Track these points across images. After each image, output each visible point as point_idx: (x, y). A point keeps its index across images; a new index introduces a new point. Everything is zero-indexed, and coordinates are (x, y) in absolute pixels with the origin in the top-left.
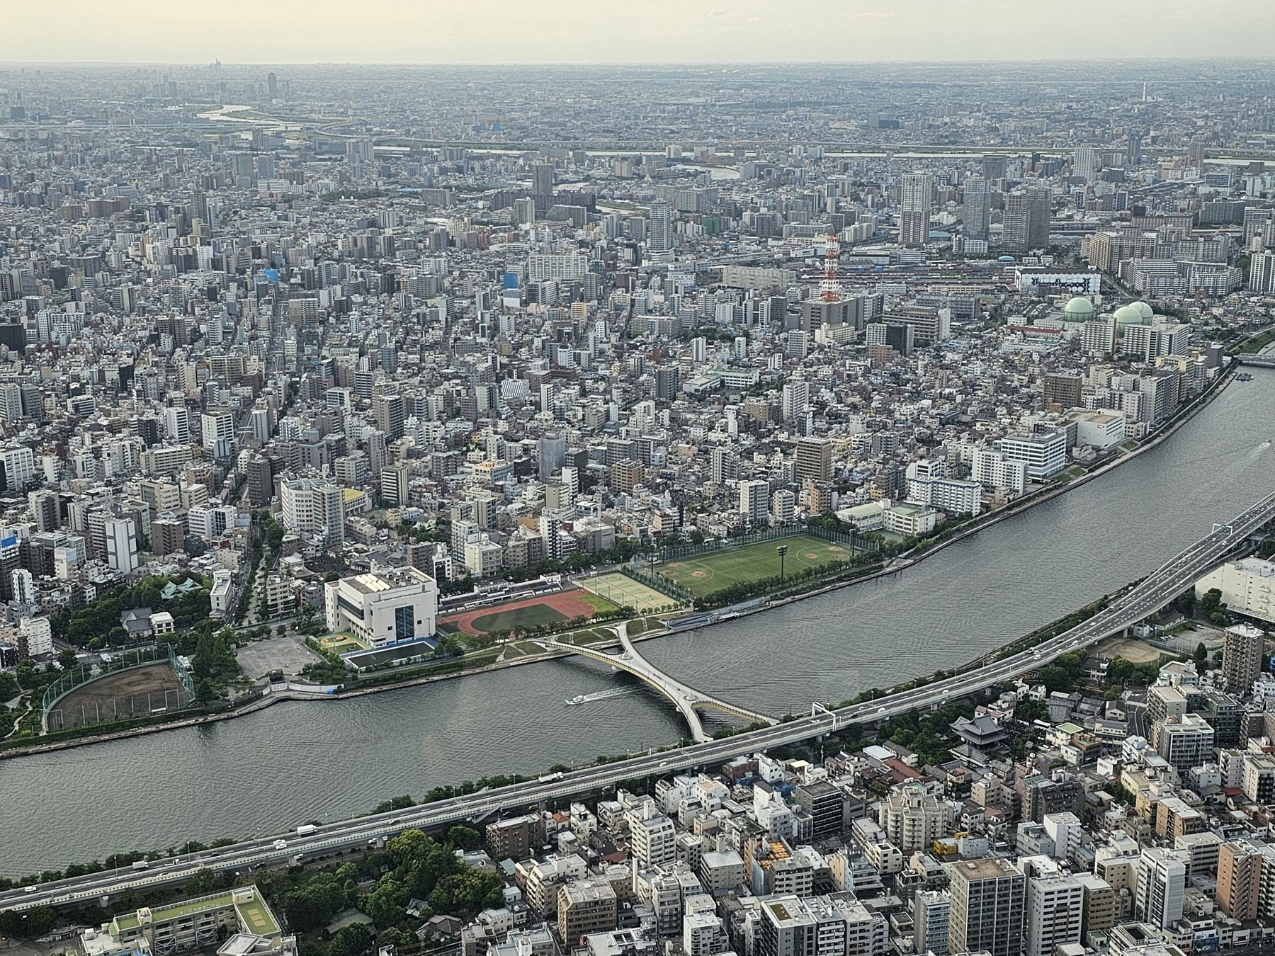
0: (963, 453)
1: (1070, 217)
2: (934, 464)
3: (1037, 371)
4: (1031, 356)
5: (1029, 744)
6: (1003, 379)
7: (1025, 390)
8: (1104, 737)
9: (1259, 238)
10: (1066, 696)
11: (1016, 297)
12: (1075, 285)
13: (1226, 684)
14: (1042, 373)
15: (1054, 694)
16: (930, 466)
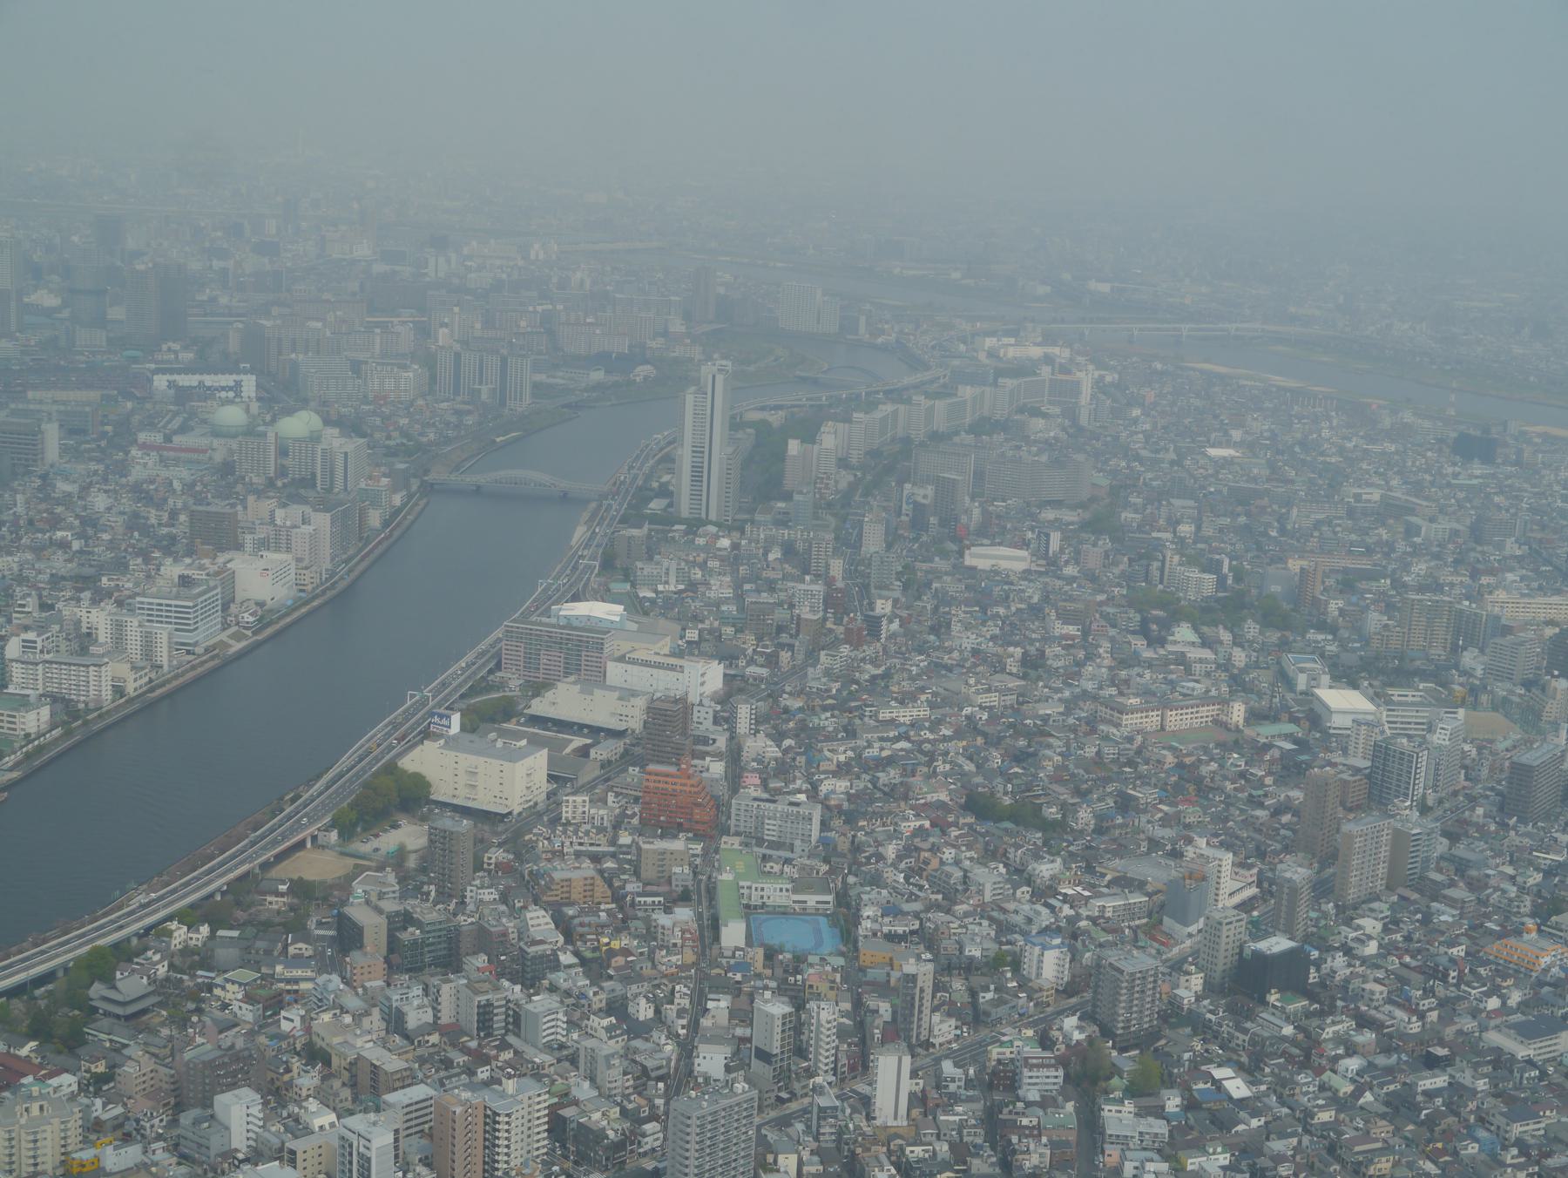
0: (84, 620)
1: (213, 300)
2: (44, 637)
3: (179, 505)
4: (171, 484)
5: (191, 1006)
6: (136, 515)
7: (165, 531)
8: (288, 981)
10: (235, 933)
11: (148, 406)
12: (223, 389)
13: (433, 894)
14: (185, 507)
15: (221, 933)
16: (39, 640)
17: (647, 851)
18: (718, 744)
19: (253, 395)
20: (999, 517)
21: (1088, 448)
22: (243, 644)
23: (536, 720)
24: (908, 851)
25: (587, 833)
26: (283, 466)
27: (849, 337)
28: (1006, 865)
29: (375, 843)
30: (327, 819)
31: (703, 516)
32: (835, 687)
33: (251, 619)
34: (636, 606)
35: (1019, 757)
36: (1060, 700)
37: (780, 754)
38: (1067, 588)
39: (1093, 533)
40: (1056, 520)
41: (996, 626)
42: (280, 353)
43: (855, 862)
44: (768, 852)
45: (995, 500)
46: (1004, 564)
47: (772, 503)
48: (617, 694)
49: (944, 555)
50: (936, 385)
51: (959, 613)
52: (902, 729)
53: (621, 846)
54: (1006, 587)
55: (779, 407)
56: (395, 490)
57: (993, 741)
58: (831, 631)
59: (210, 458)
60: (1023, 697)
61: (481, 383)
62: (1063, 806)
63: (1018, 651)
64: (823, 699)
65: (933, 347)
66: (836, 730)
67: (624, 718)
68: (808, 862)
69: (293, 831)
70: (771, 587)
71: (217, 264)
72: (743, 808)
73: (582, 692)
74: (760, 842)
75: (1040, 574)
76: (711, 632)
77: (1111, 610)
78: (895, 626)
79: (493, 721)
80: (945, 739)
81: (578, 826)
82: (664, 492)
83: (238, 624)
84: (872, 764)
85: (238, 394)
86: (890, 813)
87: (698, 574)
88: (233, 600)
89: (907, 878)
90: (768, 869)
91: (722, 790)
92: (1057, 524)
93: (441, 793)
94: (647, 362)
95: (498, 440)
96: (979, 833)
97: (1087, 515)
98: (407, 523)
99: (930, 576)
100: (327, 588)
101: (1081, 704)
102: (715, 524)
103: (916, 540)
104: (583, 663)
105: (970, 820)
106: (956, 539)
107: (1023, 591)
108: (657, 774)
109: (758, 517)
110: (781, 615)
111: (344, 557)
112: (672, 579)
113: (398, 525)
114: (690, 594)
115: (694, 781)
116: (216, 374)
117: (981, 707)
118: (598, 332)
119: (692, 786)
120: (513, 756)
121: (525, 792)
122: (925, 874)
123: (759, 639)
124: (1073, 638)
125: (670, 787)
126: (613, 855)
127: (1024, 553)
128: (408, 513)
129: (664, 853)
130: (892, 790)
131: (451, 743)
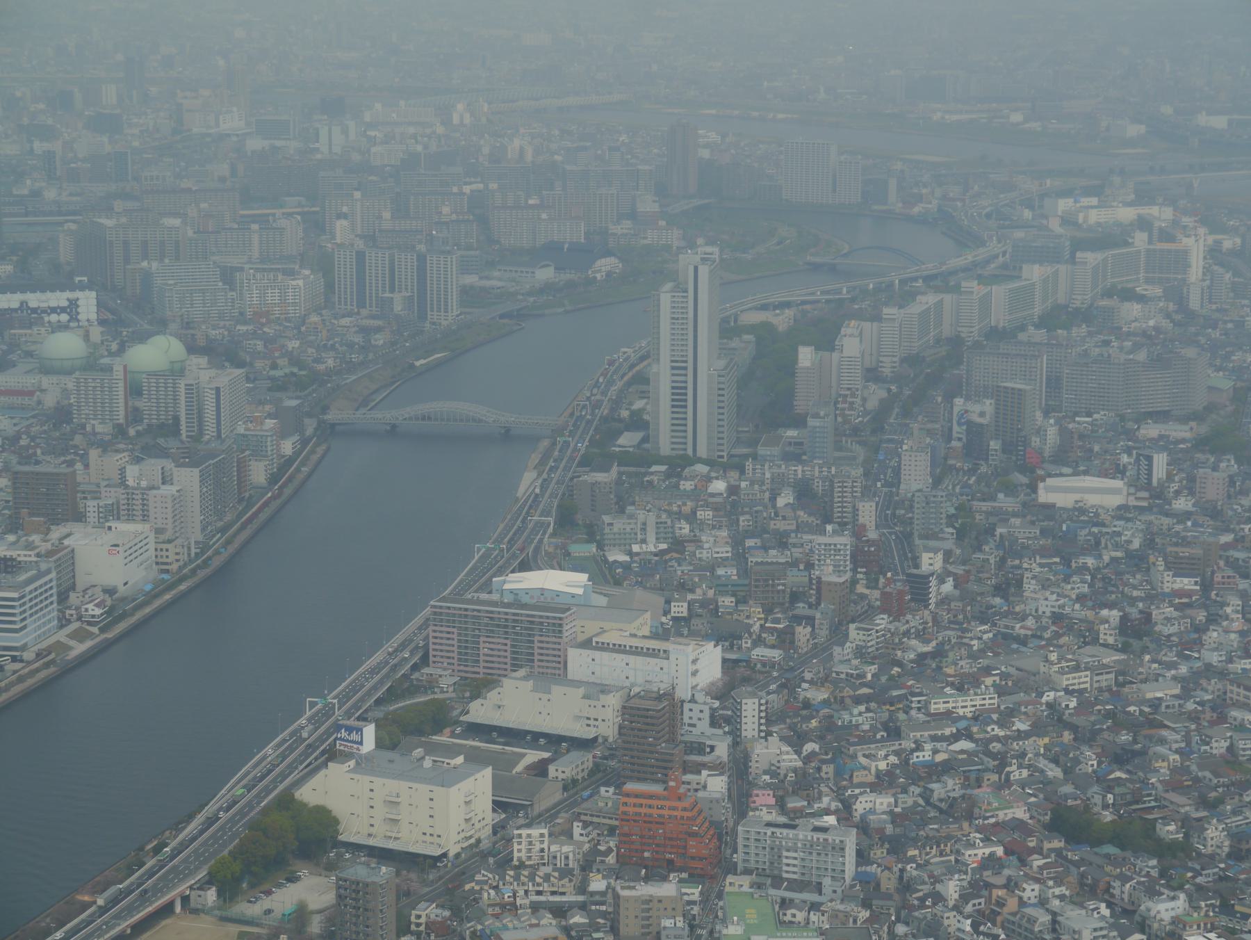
1: (36, 194)
9: (344, 223)
12: (54, 310)
17: (627, 899)
18: (717, 752)
19: (93, 317)
20: (1082, 437)
21: (1202, 340)
22: (89, 644)
23: (477, 730)
24: (976, 888)
25: (547, 878)
26: (136, 409)
27: (876, 207)
28: (1110, 905)
29: (266, 903)
30: (202, 874)
31: (690, 452)
32: (870, 671)
33: (98, 612)
34: (604, 574)
35: (1121, 758)
36: (1174, 678)
37: (799, 764)
38: (1179, 528)
39: (1212, 453)
40: (1161, 437)
41: (1083, 581)
42: (127, 260)
43: (905, 905)
44: (788, 895)
45: (1076, 414)
46: (1092, 500)
47: (780, 431)
48: (581, 691)
49: (1010, 490)
50: (993, 266)
51: (1033, 567)
52: (962, 724)
53: (592, 894)
54: (1095, 530)
55: (787, 305)
56: (283, 434)
57: (1086, 737)
58: (863, 597)
59: (39, 402)
60: (1124, 676)
61: (392, 290)
62: (1186, 823)
63: (1114, 615)
65: (988, 216)
66: (874, 729)
67: (592, 722)
68: (841, 907)
69: (157, 891)
70: (782, 542)
71: (39, 146)
72: (753, 836)
73: (535, 690)
74: (777, 881)
75: (1141, 510)
76: (704, 604)
77: (1241, 555)
78: (948, 587)
79: (421, 733)
80: (1021, 735)
81: (535, 868)
82: (638, 422)
83: (80, 618)
84: (922, 773)
85: (74, 317)
86: (949, 838)
87: (685, 529)
88: (73, 587)
89: (975, 926)
90: (788, 918)
91: (724, 813)
92: (1163, 443)
93: (352, 831)
94: (608, 253)
95: (418, 363)
96: (1071, 862)
97: (1203, 429)
98: (301, 477)
99: (992, 519)
100: (198, 567)
101: (1203, 682)
102: (709, 462)
103: (972, 471)
104: (537, 651)
105: (1058, 844)
106: (1026, 469)
107: (1119, 534)
108: (636, 796)
109: (762, 451)
110: (796, 578)
111: (220, 524)
113: (290, 479)
114: (675, 555)
115: (686, 803)
116: (43, 291)
117: (1068, 692)
118: (544, 216)
119: (685, 809)
120: (446, 779)
121: (463, 826)
122: (999, 919)
123: (768, 611)
124: (1189, 594)
125: (655, 812)
126: (583, 907)
127: (1118, 484)
128: (303, 464)
129: (649, 900)
130: (951, 806)
131: (365, 765)
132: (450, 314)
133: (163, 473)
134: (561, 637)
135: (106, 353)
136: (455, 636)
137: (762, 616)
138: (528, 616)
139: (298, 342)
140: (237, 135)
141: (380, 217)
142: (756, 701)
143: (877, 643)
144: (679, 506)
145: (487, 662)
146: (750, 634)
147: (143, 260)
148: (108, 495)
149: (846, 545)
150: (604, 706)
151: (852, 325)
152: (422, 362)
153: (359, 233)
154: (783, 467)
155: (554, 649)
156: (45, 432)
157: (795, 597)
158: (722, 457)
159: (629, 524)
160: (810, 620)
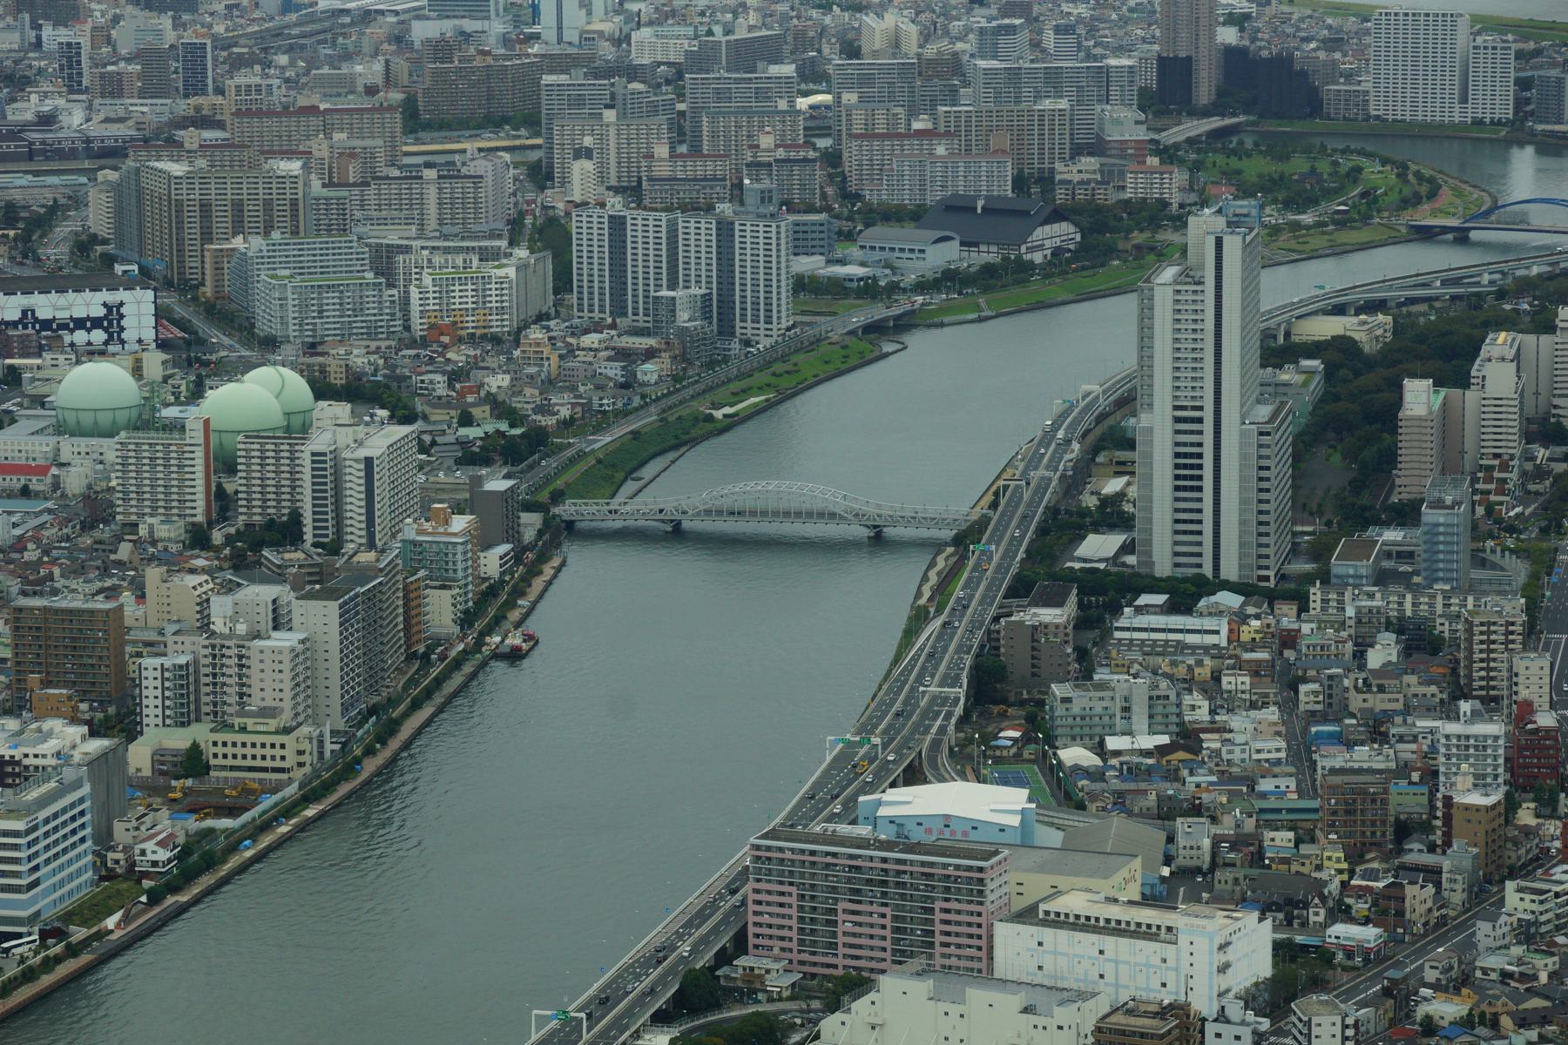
1: (47, 121)
12: (80, 324)
19: (149, 335)
31: (1208, 570)
33: (163, 855)
47: (1372, 532)
58: (1527, 832)
59: (56, 485)
61: (672, 286)
64: (1516, 997)
70: (1377, 731)
87: (1198, 709)
94: (1057, 215)
104: (938, 927)
110: (1406, 799)
112: (1140, 719)
114: (1181, 755)
123: (1355, 856)
132: (774, 326)
133: (274, 611)
134: (981, 903)
135: (172, 399)
136: (793, 900)
137: (1345, 866)
138: (923, 864)
139: (507, 377)
140: (396, 13)
141: (649, 156)
142: (1338, 1020)
143: (1558, 917)
144: (1190, 668)
145: (851, 946)
146: (1323, 899)
147: (235, 234)
148: (179, 647)
149: (1496, 738)
150: (1060, 1028)
151: (1500, 341)
152: (728, 410)
153: (613, 182)
154: (1378, 596)
155: (970, 924)
156: (68, 539)
157: (1404, 830)
158: (1267, 579)
159: (1102, 699)
160: (1433, 875)
